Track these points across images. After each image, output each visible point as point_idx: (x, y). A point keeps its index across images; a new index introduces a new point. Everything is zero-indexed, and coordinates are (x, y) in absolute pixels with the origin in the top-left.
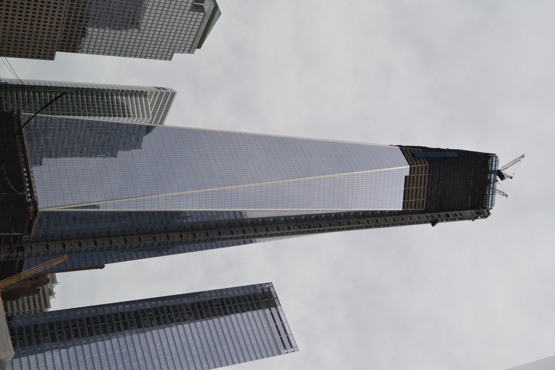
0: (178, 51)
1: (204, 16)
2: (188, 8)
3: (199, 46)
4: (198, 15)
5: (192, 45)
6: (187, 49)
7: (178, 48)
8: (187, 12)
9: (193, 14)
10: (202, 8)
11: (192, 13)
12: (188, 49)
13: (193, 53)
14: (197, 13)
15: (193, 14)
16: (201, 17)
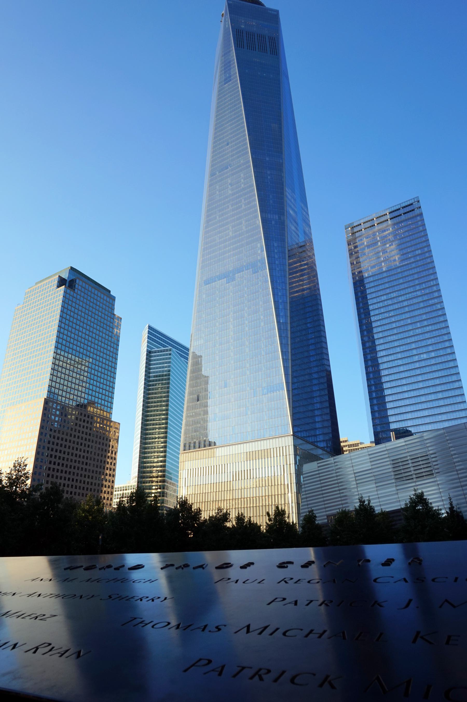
0: (113, 309)
1: (80, 279)
2: (72, 293)
3: (110, 291)
4: (79, 285)
5: (107, 296)
6: (111, 301)
7: (110, 310)
8: (75, 295)
9: (78, 289)
10: (72, 280)
11: (76, 290)
12: (111, 301)
13: (115, 297)
14: (77, 286)
15: (78, 289)
16: (81, 283)
